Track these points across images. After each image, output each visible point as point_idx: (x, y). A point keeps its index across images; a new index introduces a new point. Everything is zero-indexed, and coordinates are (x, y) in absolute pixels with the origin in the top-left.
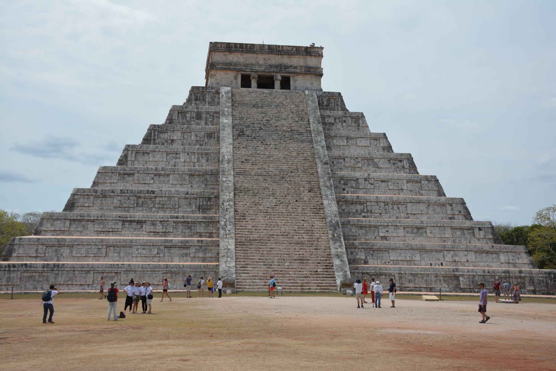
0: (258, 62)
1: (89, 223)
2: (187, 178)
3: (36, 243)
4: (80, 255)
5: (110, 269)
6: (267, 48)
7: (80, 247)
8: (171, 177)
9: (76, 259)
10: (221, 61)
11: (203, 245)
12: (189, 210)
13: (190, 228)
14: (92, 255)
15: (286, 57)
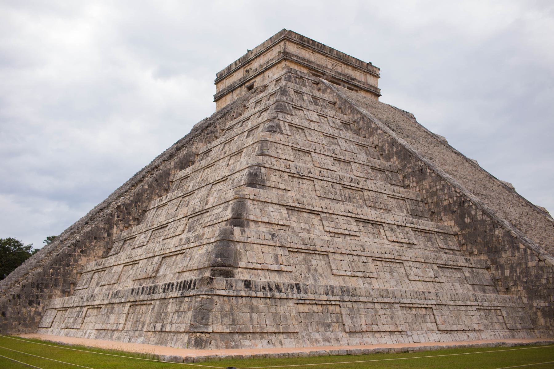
0: (327, 65)
1: (313, 216)
2: (370, 171)
3: (271, 243)
4: (344, 273)
5: (418, 301)
6: (335, 53)
7: (338, 257)
8: (353, 166)
9: (340, 279)
10: (294, 53)
11: (473, 266)
12: (402, 214)
13: (429, 240)
14: (360, 274)
15: (350, 68)
